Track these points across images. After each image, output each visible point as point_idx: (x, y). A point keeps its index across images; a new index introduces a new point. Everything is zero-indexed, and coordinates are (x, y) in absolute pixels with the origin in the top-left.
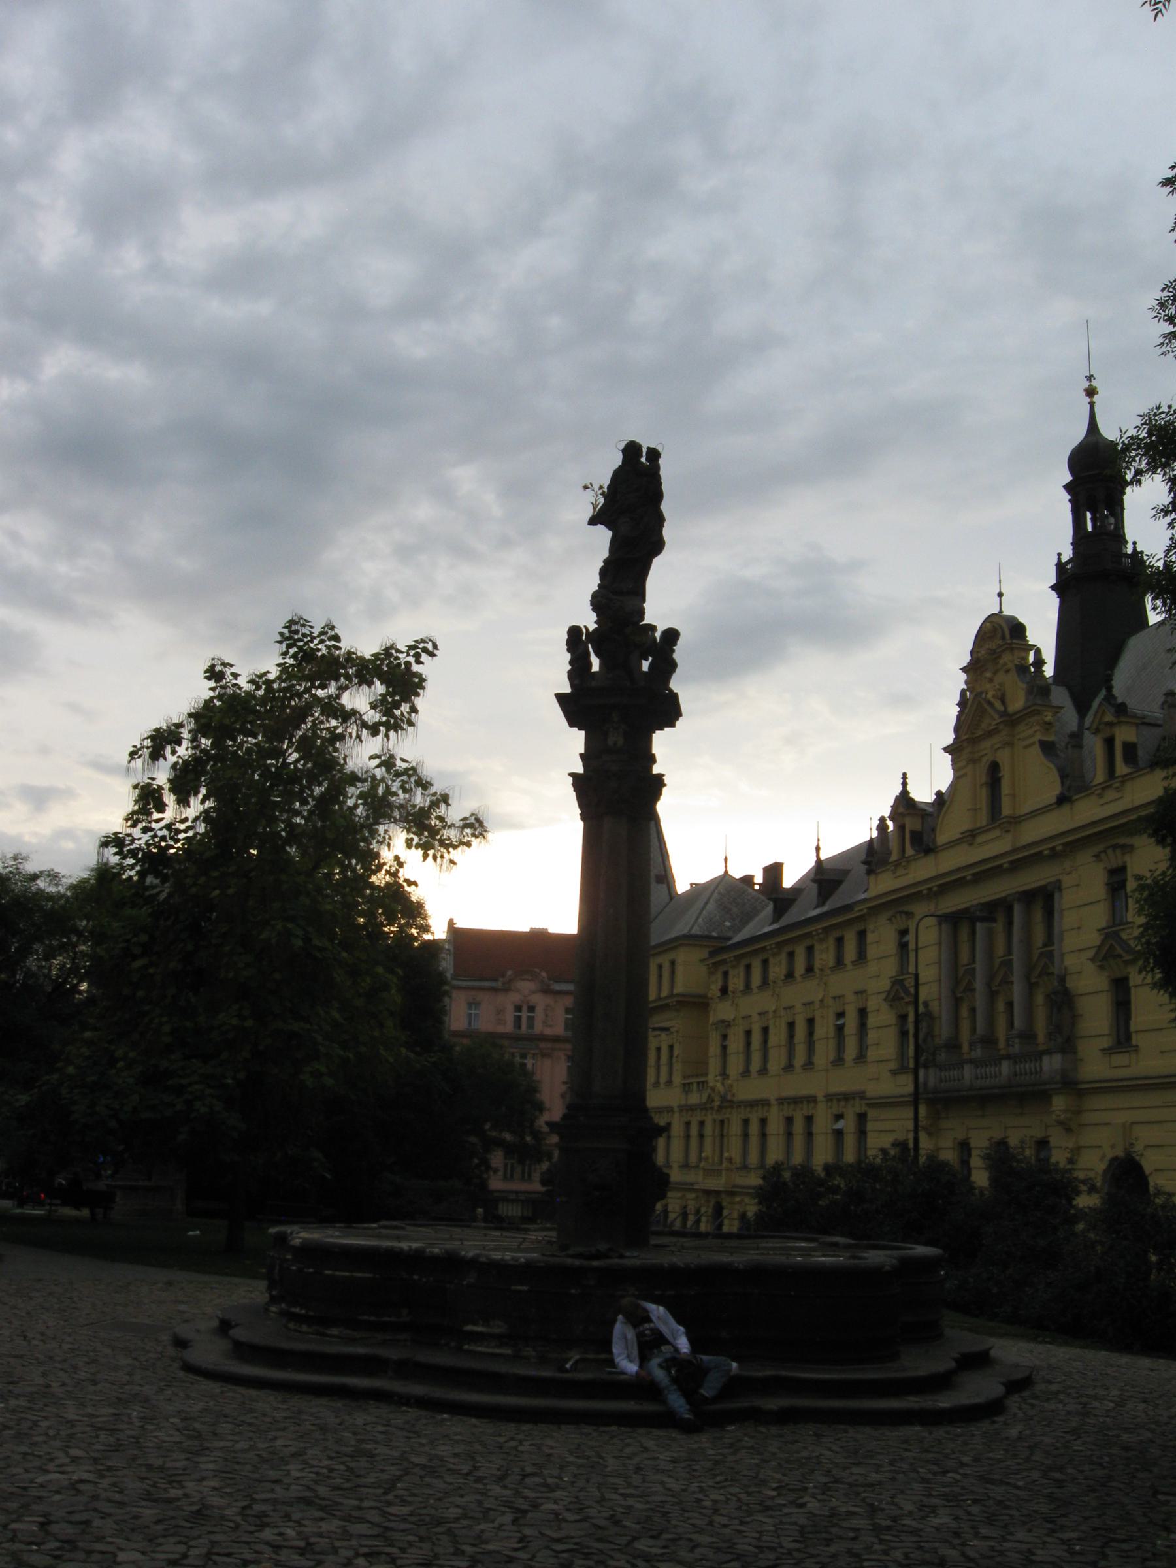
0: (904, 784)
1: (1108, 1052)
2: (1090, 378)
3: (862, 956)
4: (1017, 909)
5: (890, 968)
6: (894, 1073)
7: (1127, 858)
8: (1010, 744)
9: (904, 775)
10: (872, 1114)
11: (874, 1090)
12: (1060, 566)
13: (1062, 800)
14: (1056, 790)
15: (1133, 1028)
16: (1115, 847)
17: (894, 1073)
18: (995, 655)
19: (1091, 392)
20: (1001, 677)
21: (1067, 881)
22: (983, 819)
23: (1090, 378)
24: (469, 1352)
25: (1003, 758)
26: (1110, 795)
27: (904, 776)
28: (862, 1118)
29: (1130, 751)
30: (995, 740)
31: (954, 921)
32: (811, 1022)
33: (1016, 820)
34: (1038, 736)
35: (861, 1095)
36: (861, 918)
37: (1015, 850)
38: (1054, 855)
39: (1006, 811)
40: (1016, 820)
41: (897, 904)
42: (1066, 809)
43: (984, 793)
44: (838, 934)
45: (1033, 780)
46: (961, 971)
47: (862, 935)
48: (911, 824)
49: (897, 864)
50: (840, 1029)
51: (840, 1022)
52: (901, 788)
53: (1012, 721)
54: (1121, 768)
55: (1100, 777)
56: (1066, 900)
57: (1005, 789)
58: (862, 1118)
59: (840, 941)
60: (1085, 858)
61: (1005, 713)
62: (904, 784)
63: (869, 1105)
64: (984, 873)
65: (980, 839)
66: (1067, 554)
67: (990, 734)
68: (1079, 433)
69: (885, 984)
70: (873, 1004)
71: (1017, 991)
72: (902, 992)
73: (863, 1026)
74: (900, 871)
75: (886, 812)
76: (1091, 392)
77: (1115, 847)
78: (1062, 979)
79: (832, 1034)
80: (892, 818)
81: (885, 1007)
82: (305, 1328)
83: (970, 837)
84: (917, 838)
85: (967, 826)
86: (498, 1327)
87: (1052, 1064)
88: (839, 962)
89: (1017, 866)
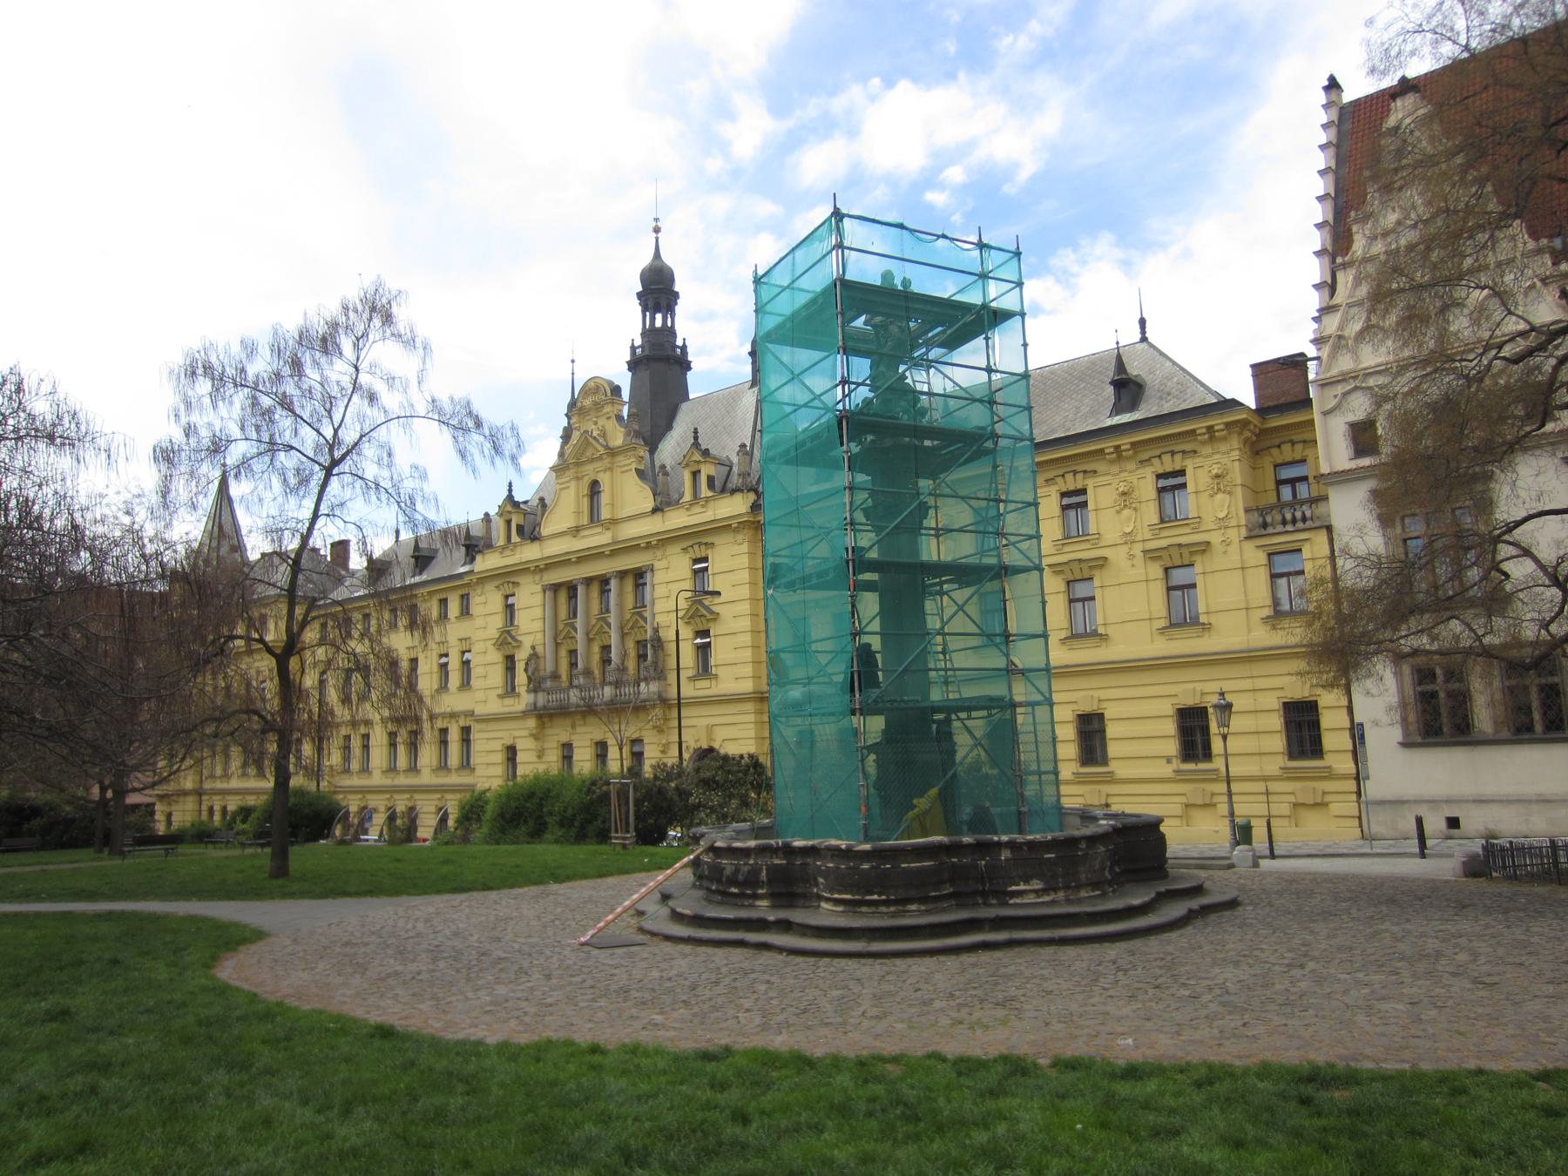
0: (510, 490)
1: (692, 679)
2: (656, 220)
3: (465, 612)
4: (613, 584)
5: (497, 622)
6: (501, 697)
7: (709, 552)
8: (611, 469)
9: (510, 485)
10: (475, 727)
11: (480, 710)
12: (633, 348)
13: (655, 510)
14: (650, 505)
15: (712, 662)
16: (700, 544)
17: (501, 697)
18: (598, 406)
19: (657, 230)
20: (601, 422)
21: (657, 565)
22: (585, 520)
23: (656, 220)
24: (1015, 905)
25: (605, 480)
26: (697, 509)
27: (510, 485)
28: (466, 731)
29: (711, 480)
30: (598, 465)
31: (555, 588)
32: (414, 661)
33: (614, 522)
34: (634, 466)
35: (470, 714)
36: (468, 585)
37: (614, 543)
38: (649, 546)
39: (605, 514)
40: (614, 522)
41: (507, 578)
42: (658, 517)
43: (586, 501)
44: (443, 596)
45: (629, 495)
46: (561, 627)
47: (465, 599)
48: (516, 520)
49: (504, 548)
50: (444, 666)
51: (444, 660)
52: (506, 493)
53: (613, 452)
54: (705, 491)
55: (687, 497)
56: (659, 577)
57: (605, 498)
58: (466, 731)
59: (444, 602)
60: (674, 549)
61: (607, 447)
62: (510, 490)
63: (478, 721)
64: (584, 558)
65: (583, 533)
66: (638, 342)
67: (593, 460)
68: (646, 259)
69: (493, 632)
70: (477, 648)
71: (614, 640)
72: (507, 640)
73: (466, 664)
74: (507, 552)
75: (493, 511)
76: (657, 230)
77: (700, 544)
78: (656, 630)
79: (436, 668)
80: (500, 514)
81: (492, 649)
82: (883, 909)
83: (576, 531)
84: (520, 529)
85: (571, 524)
86: (1037, 885)
87: (648, 689)
88: (444, 616)
89: (614, 553)
